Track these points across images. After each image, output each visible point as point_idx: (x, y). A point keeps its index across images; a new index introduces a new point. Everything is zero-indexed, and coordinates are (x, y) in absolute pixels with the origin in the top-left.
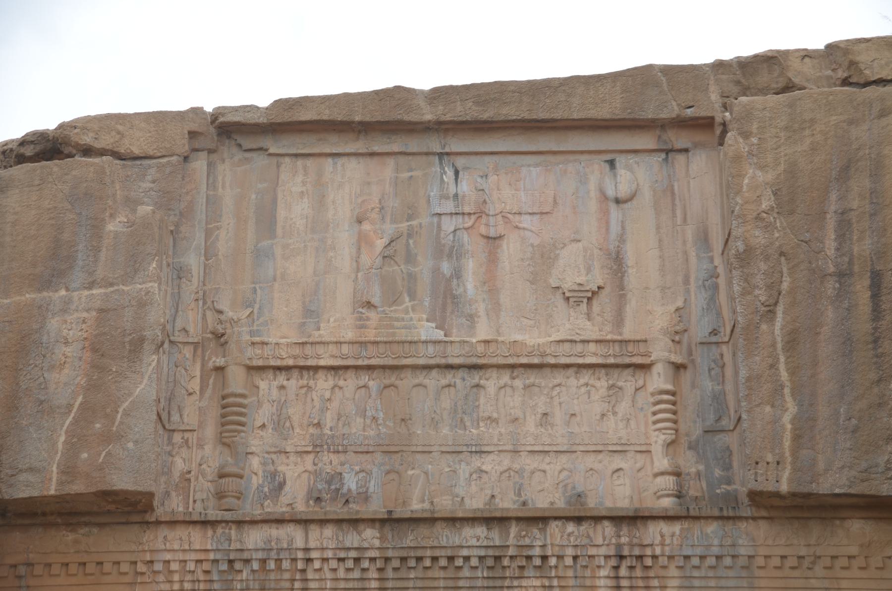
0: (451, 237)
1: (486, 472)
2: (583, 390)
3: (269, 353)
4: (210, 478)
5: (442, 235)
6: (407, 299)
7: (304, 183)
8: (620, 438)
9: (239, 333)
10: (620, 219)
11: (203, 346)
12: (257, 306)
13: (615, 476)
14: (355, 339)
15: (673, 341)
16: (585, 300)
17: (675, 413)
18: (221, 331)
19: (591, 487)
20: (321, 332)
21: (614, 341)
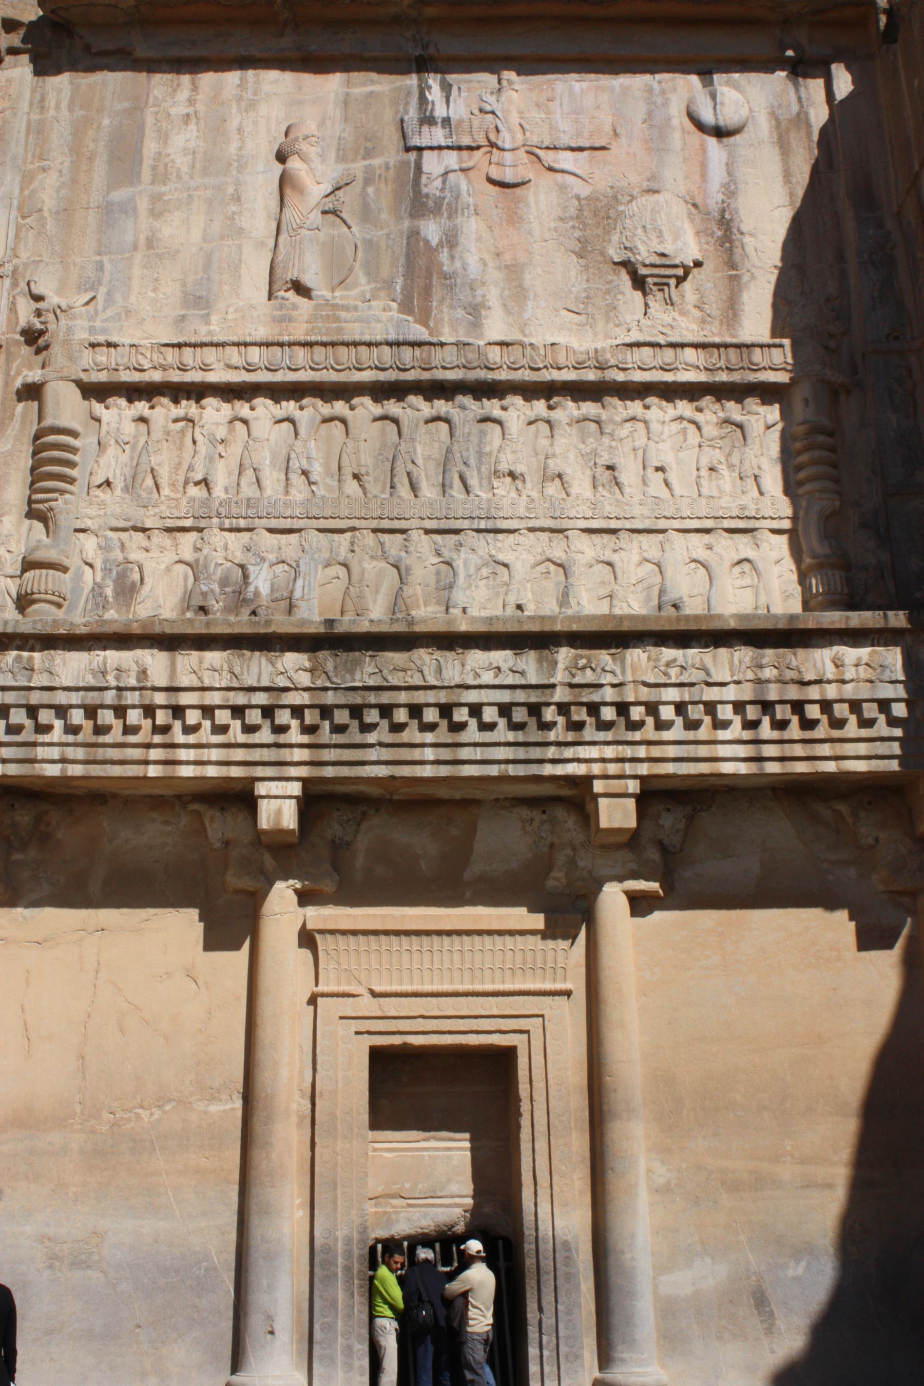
0: (438, 183)
1: (506, 565)
2: (676, 427)
3: (120, 361)
4: (10, 571)
5: (424, 179)
6: (363, 279)
7: (191, 102)
8: (743, 508)
9: (69, 329)
10: (724, 160)
11: (9, 354)
12: (103, 290)
13: (737, 569)
14: (270, 339)
15: (826, 348)
16: (673, 282)
17: (835, 466)
18: (39, 326)
19: (695, 592)
20: (212, 328)
21: (726, 346)
